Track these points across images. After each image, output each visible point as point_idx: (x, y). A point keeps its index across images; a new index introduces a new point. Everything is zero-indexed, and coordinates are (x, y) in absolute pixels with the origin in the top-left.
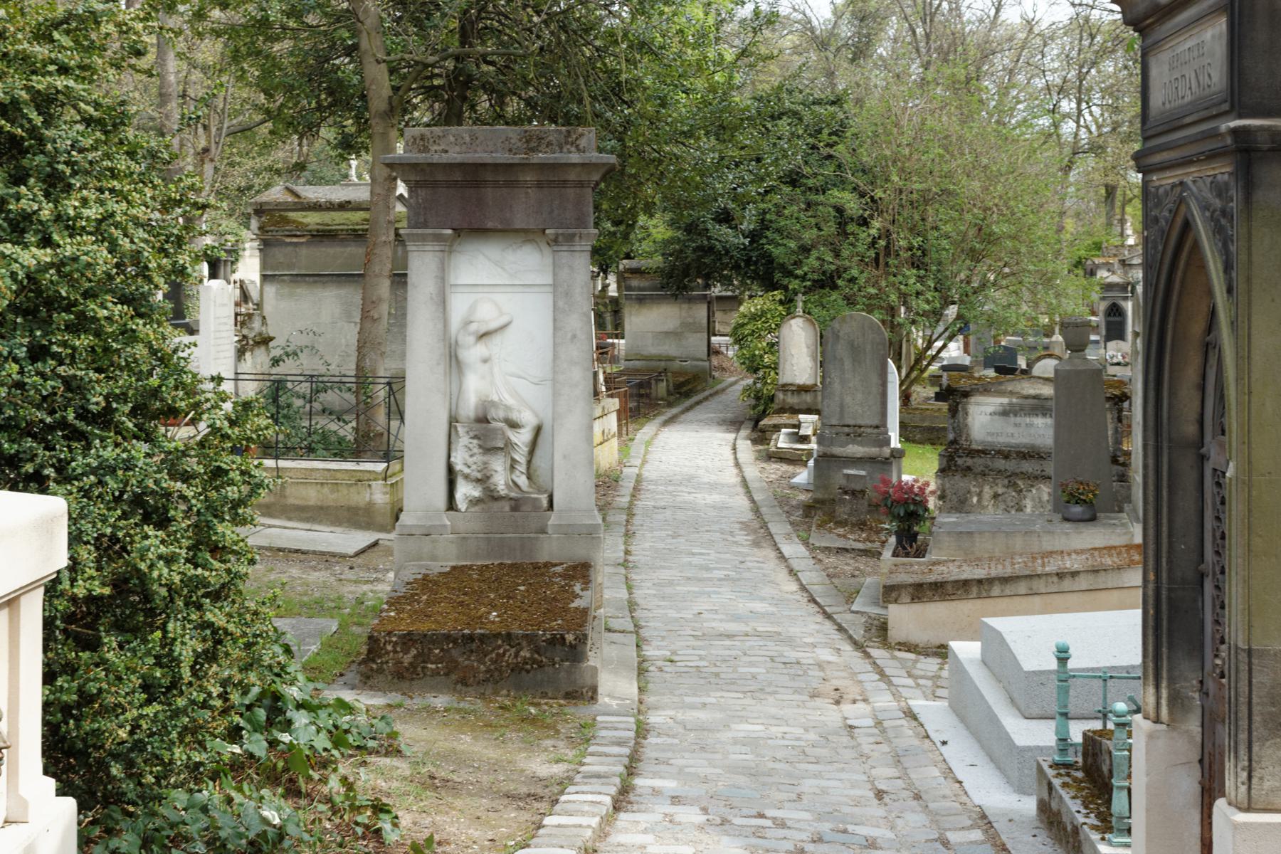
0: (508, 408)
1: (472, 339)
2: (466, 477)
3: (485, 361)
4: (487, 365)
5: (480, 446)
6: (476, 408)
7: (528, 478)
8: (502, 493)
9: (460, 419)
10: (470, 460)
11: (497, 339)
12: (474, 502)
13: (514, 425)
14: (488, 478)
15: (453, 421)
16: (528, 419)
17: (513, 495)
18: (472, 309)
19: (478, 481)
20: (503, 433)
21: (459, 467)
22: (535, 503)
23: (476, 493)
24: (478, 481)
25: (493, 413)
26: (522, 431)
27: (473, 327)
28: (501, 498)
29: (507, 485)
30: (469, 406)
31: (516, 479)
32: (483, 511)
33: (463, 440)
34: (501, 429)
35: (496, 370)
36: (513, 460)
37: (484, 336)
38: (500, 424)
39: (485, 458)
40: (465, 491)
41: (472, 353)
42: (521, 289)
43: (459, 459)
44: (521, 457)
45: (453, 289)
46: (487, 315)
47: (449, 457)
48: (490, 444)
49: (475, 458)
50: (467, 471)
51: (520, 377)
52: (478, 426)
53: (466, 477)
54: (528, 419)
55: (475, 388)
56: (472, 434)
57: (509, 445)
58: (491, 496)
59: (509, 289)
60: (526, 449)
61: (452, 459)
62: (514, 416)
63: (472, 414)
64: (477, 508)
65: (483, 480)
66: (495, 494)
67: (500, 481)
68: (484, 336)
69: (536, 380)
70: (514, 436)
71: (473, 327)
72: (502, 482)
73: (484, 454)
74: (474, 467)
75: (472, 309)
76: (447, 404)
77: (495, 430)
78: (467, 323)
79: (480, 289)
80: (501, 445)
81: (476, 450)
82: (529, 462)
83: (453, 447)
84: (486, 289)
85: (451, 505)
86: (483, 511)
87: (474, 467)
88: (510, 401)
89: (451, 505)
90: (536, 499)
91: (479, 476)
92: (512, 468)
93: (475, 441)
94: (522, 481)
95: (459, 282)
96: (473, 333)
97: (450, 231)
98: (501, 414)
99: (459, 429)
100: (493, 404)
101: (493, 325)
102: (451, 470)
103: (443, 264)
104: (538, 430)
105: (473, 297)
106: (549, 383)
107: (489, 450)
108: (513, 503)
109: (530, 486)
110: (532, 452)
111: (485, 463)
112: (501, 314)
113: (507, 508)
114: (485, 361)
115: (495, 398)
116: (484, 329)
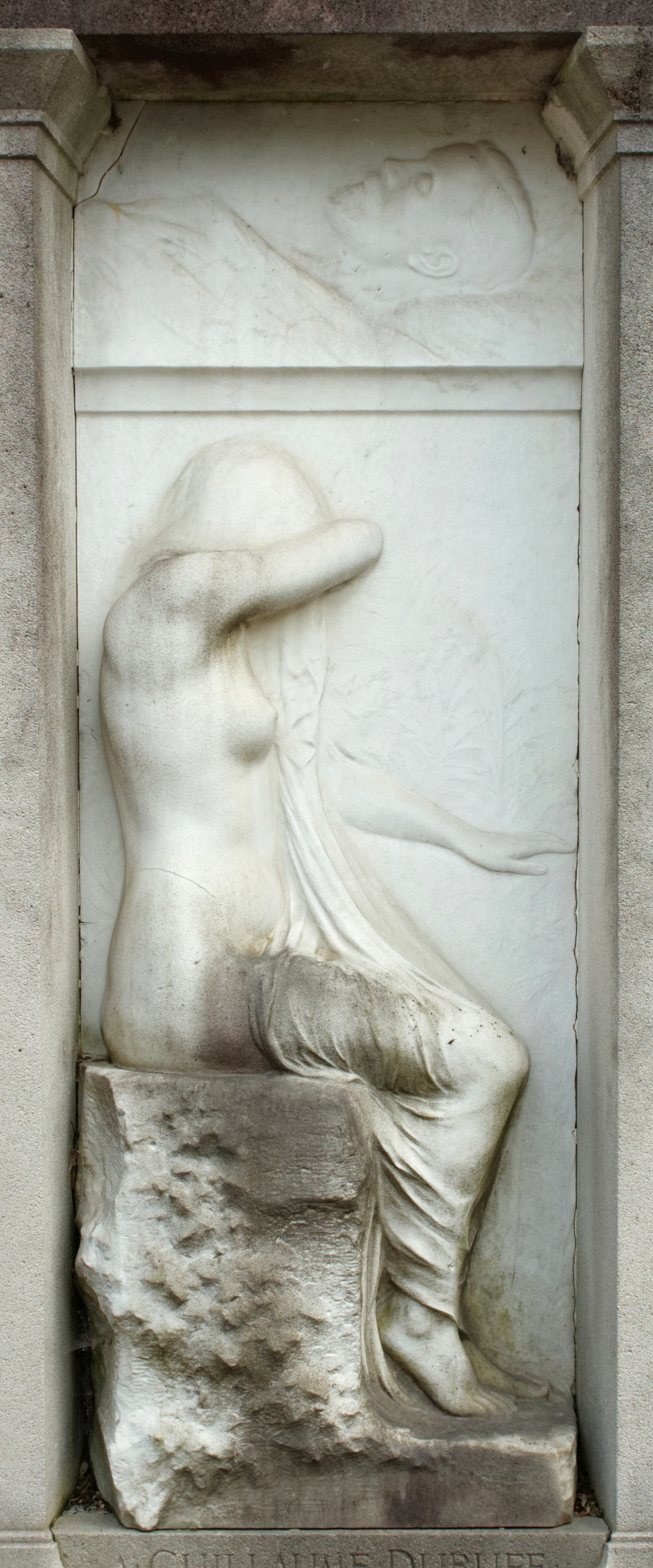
0: (370, 993)
1: (183, 638)
2: (163, 1352)
3: (251, 752)
4: (260, 773)
5: (233, 1195)
6: (210, 992)
7: (463, 1336)
8: (347, 1434)
9: (126, 1047)
10: (181, 1268)
11: (305, 645)
12: (196, 1480)
13: (405, 1081)
14: (277, 1360)
15: (91, 1049)
16: (472, 1044)
17: (402, 1439)
18: (185, 491)
19: (220, 1372)
20: (353, 1126)
21: (124, 1297)
22: (515, 1491)
23: (214, 1437)
24: (220, 1372)
25: (293, 1020)
26: (444, 1108)
27: (190, 577)
28: (343, 1459)
29: (370, 1383)
30: (175, 981)
31: (406, 1347)
32: (249, 1520)
33: (149, 1160)
34: (340, 1103)
35: (303, 798)
36: (397, 1256)
37: (247, 622)
38: (335, 1078)
39: (259, 1258)
40: (154, 1422)
41: (189, 709)
42: (423, 395)
43: (124, 1256)
44: (432, 1245)
45: (89, 396)
46: (264, 513)
47: (73, 1239)
48: (282, 1185)
49: (203, 1258)
50: (164, 1320)
51: (415, 836)
52: (223, 1084)
53: (163, 1352)
54: (472, 1044)
55: (207, 885)
56: (187, 1129)
57: (386, 1179)
58: (286, 1446)
59: (367, 395)
60: (461, 1201)
61: (89, 1256)
62: (407, 1034)
63: (187, 1026)
64: (216, 1508)
65: (252, 1371)
66: (313, 1443)
67: (336, 1374)
68: (247, 622)
69: (496, 854)
70: (392, 1131)
71: (190, 577)
72: (349, 1379)
73: (253, 1234)
74: (201, 1302)
75: (185, 491)
76: (63, 971)
77: (312, 1107)
78: (155, 563)
79: (219, 395)
80: (339, 1186)
81: (209, 1215)
82: (468, 1258)
83: (93, 1188)
84: (249, 396)
85: (86, 1485)
86: (249, 1520)
87: (201, 1302)
88: (378, 955)
89: (86, 1485)
90: (519, 1463)
91: (229, 1350)
92: (391, 1293)
93: (206, 1168)
94: (441, 1357)
95: (118, 356)
96: (191, 607)
97: (63, 40)
98: (339, 1025)
99: (123, 1101)
100: (291, 968)
101: (293, 571)
102: (79, 1303)
103: (29, 228)
104: (515, 1100)
105: (191, 435)
106: (558, 866)
107: (279, 1214)
108: (402, 1481)
109: (479, 1383)
110: (479, 1212)
111: (259, 1284)
112: (329, 521)
113: (372, 1510)
114: (251, 752)
115: (303, 941)
116: (242, 588)
